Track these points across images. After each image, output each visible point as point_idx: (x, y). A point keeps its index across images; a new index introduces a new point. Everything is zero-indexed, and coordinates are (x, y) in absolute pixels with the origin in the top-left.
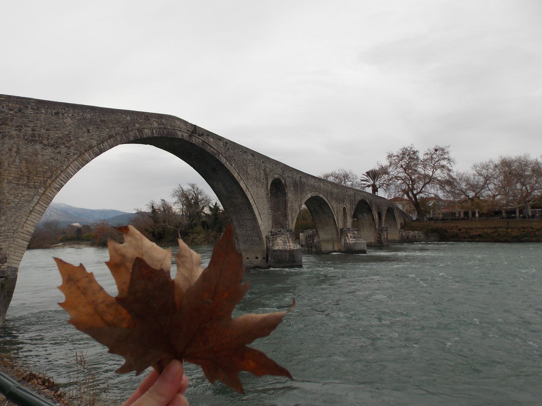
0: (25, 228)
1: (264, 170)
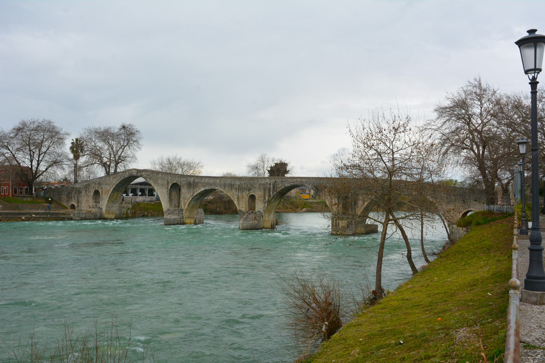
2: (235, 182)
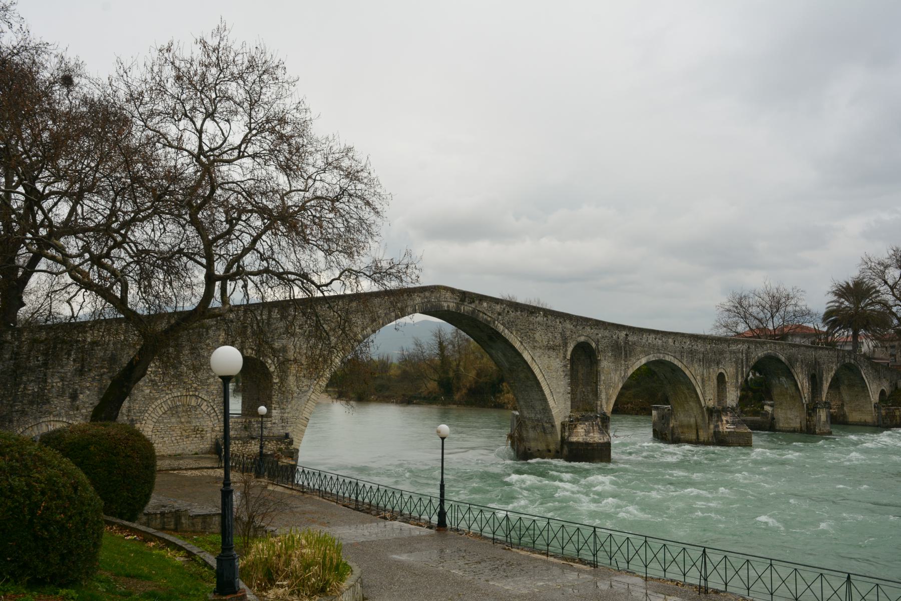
0: (304, 415)
1: (561, 333)
2: (697, 345)
